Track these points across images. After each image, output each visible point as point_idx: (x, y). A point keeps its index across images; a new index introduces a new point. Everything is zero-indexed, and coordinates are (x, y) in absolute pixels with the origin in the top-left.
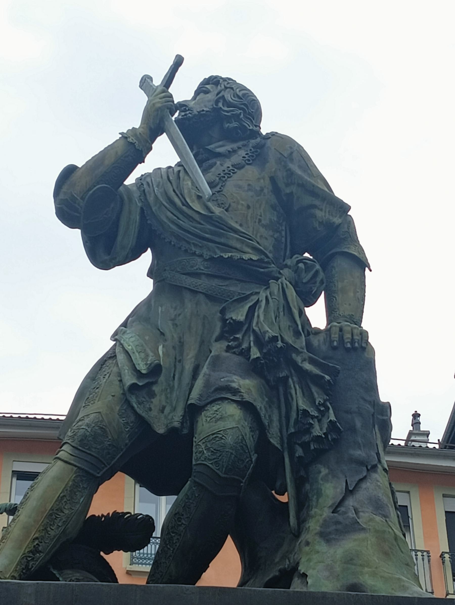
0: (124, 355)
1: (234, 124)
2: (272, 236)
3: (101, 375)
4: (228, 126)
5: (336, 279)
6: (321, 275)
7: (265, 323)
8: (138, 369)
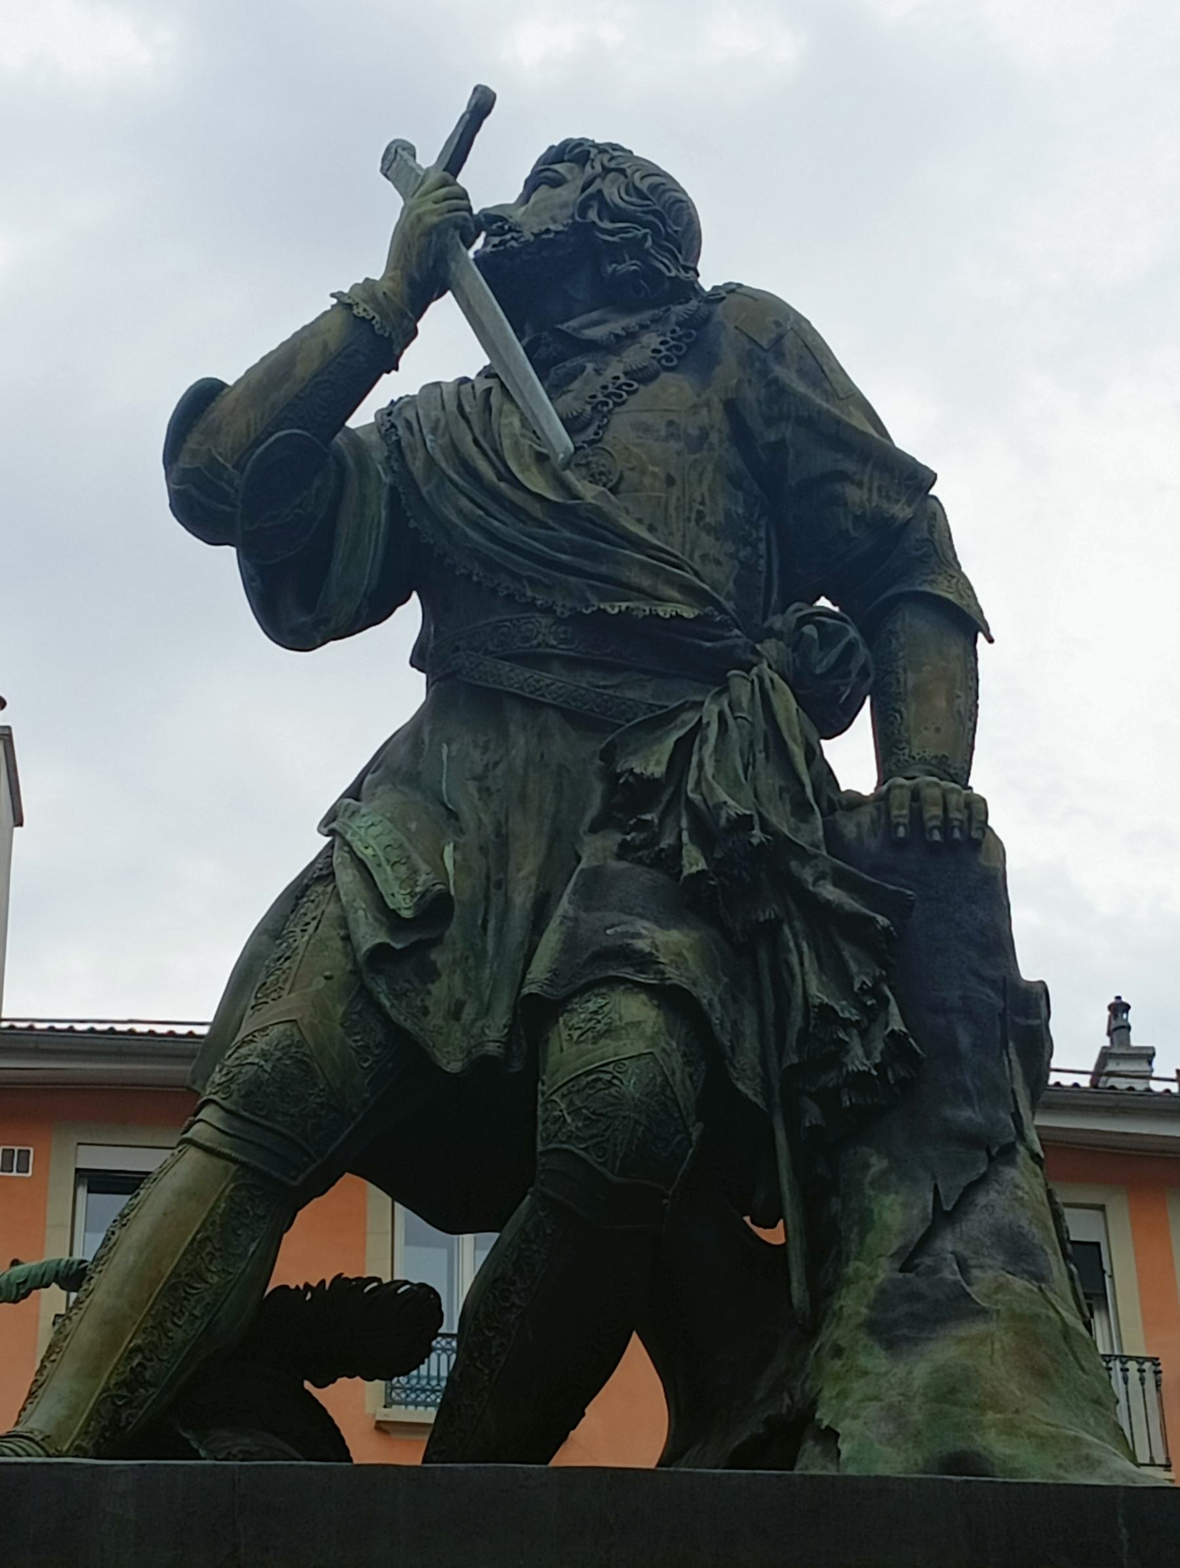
0: (356, 873)
1: (630, 266)
2: (733, 556)
3: (295, 926)
4: (615, 270)
5: (901, 662)
6: (863, 651)
7: (718, 783)
8: (392, 907)
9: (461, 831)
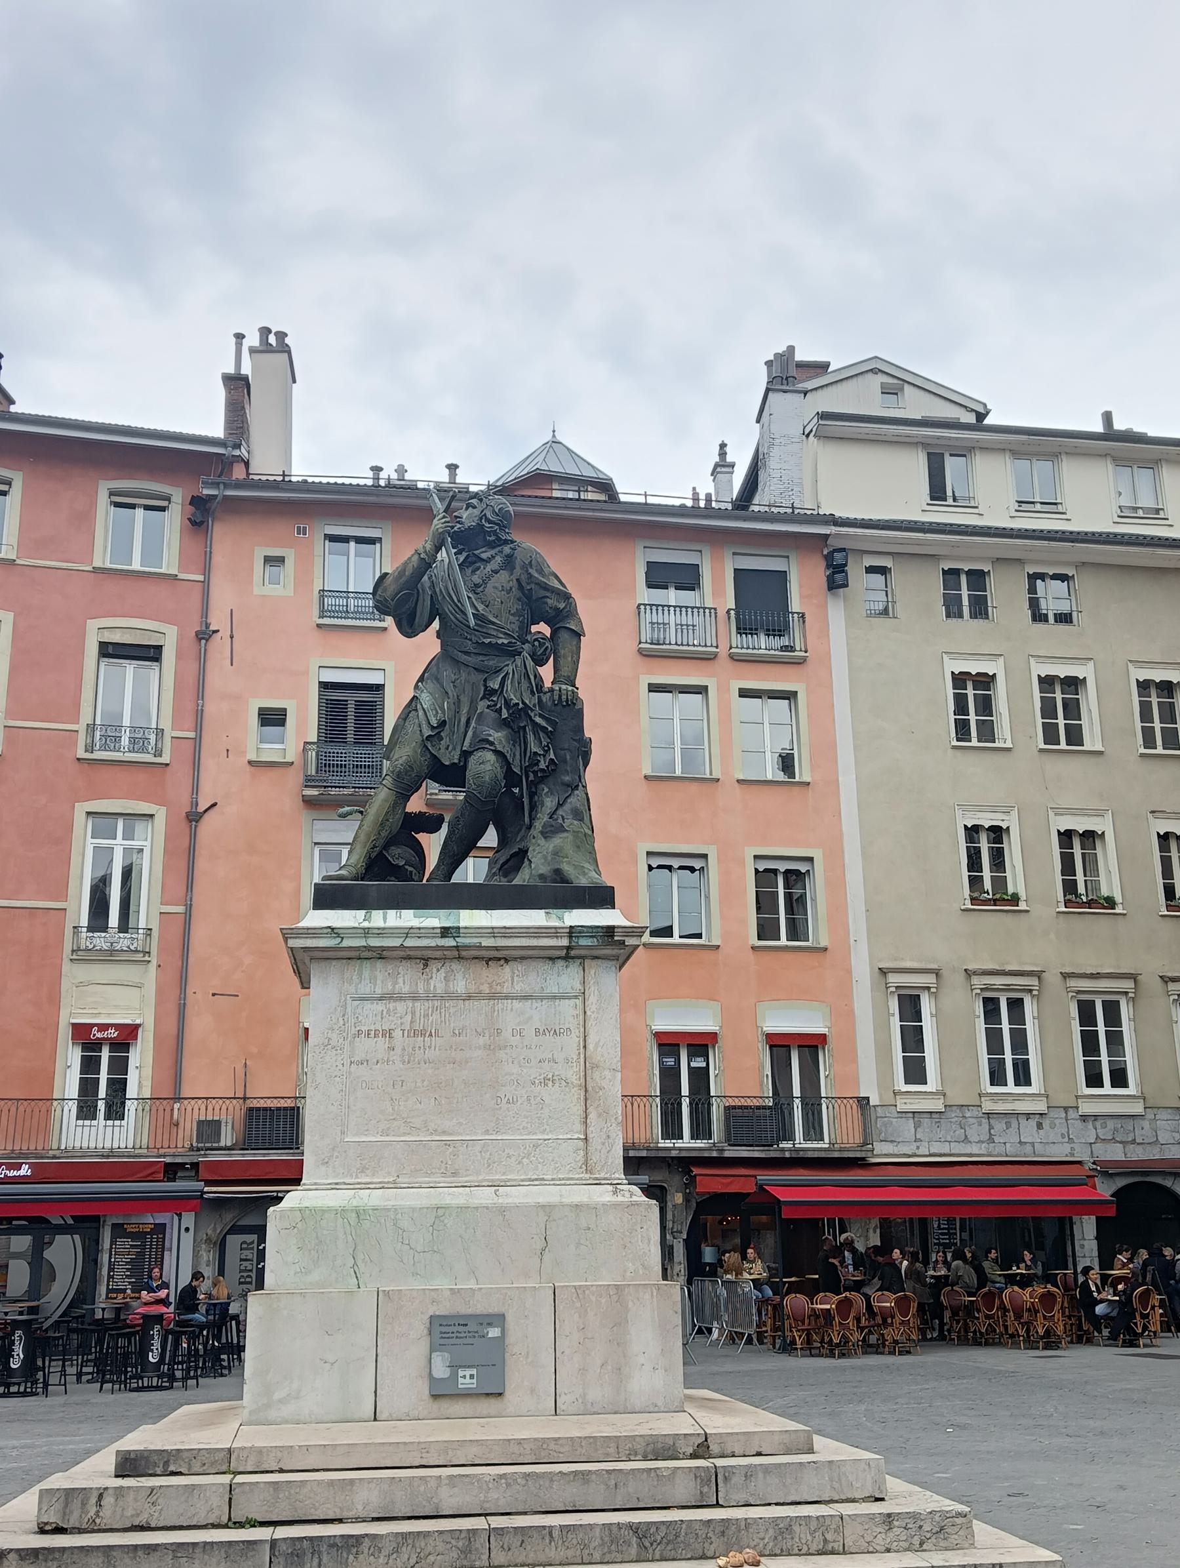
9: (449, 698)
